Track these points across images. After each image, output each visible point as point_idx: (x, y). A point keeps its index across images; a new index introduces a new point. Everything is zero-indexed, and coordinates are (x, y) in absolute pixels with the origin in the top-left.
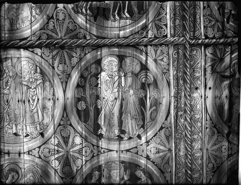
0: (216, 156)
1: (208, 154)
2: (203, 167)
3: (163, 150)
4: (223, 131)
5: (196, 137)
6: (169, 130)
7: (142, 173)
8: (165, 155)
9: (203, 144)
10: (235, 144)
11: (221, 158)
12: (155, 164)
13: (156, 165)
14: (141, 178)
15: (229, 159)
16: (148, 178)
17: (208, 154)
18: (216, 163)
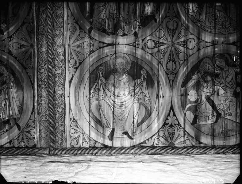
0: (79, 52)
1: (70, 50)
2: (65, 63)
3: (25, 45)
4: (85, 27)
5: (58, 32)
6: (31, 25)
7: (4, 69)
8: (26, 52)
9: (65, 40)
10: (97, 40)
11: (83, 54)
12: (17, 59)
13: (18, 61)
14: (3, 73)
15: (91, 55)
16: (10, 74)
17: (69, 50)
18: (78, 59)
